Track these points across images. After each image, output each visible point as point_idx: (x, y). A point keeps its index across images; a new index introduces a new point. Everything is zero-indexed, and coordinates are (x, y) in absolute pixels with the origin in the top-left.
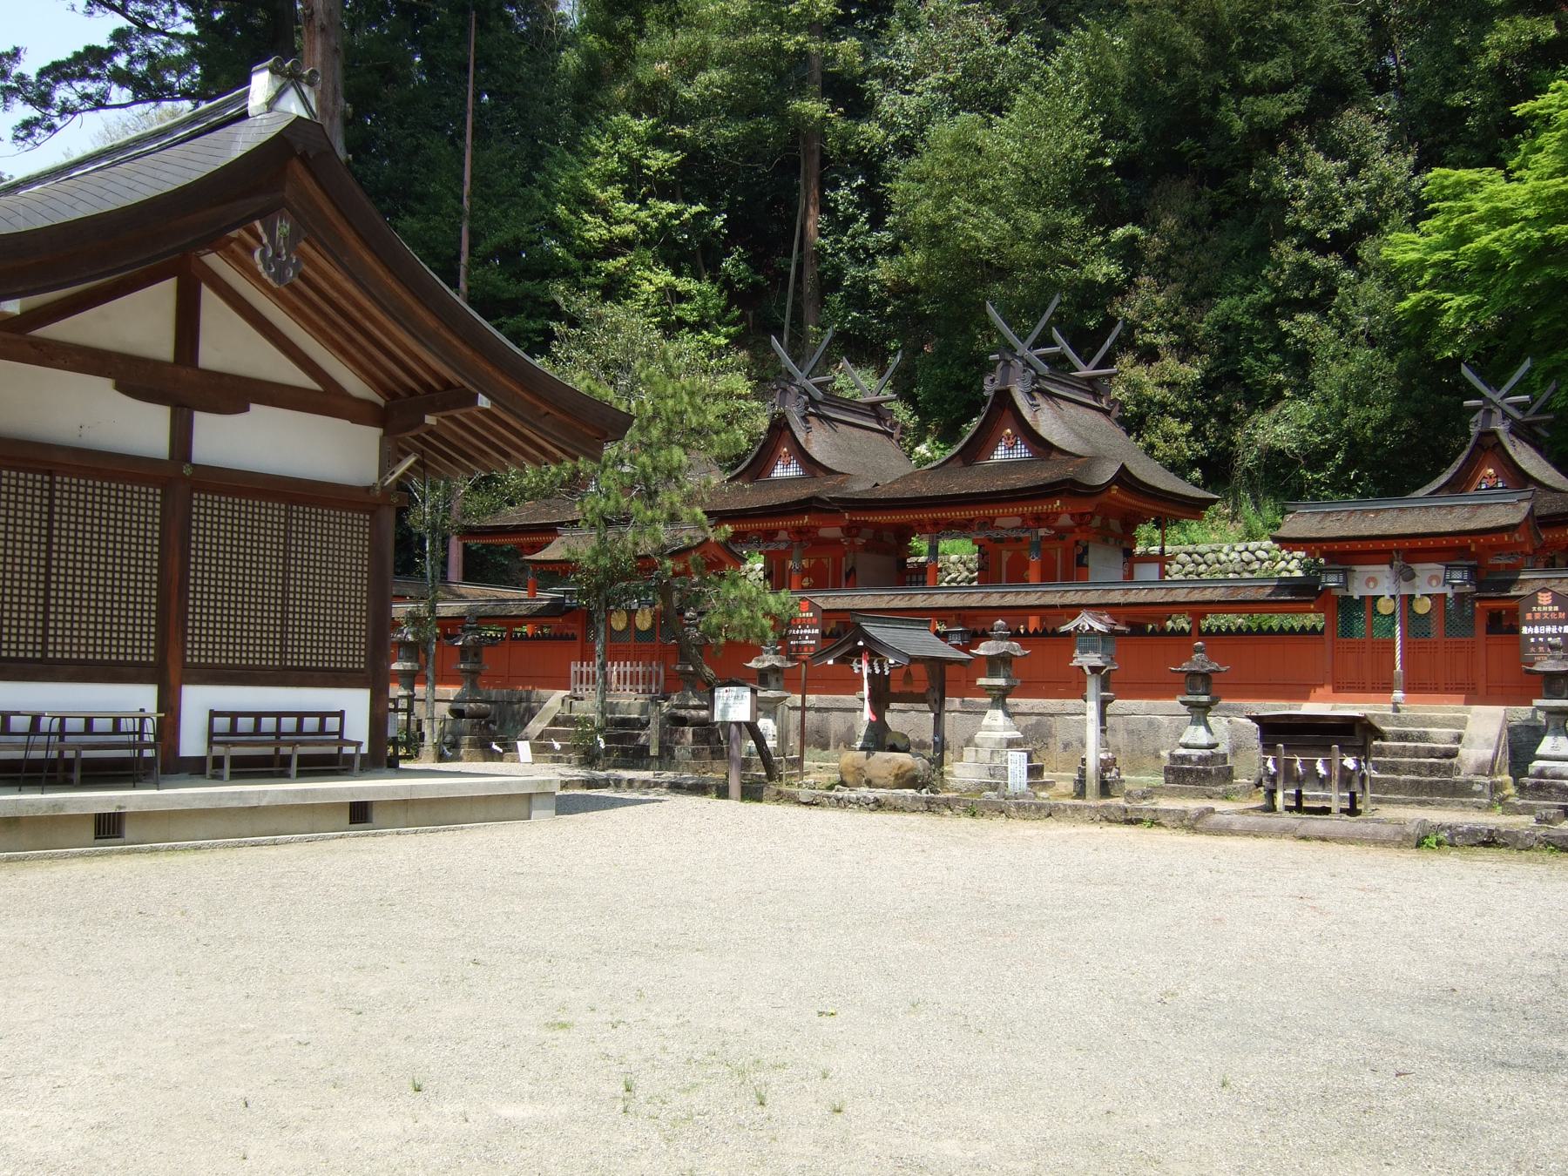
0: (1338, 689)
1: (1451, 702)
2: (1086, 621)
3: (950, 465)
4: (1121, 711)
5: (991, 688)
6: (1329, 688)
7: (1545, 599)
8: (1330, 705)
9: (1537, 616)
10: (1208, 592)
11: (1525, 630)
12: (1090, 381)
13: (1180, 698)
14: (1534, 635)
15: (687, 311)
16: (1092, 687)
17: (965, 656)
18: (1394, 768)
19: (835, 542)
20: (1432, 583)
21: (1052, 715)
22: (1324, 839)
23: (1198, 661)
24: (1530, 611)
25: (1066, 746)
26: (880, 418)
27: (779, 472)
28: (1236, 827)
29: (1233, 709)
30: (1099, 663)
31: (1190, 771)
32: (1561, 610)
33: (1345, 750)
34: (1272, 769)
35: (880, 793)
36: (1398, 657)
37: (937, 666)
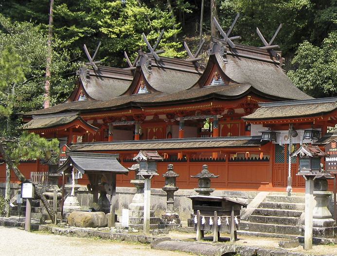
0: (274, 185)
2: (142, 156)
3: (194, 88)
5: (135, 184)
8: (268, 193)
12: (269, 50)
13: (195, 189)
14: (332, 162)
15: (156, 23)
17: (125, 170)
18: (276, 221)
19: (162, 121)
21: (180, 196)
23: (205, 172)
25: (184, 209)
26: (196, 69)
27: (141, 91)
29: (237, 194)
30: (146, 174)
33: (219, 214)
35: (73, 229)
36: (290, 170)
37: (114, 174)
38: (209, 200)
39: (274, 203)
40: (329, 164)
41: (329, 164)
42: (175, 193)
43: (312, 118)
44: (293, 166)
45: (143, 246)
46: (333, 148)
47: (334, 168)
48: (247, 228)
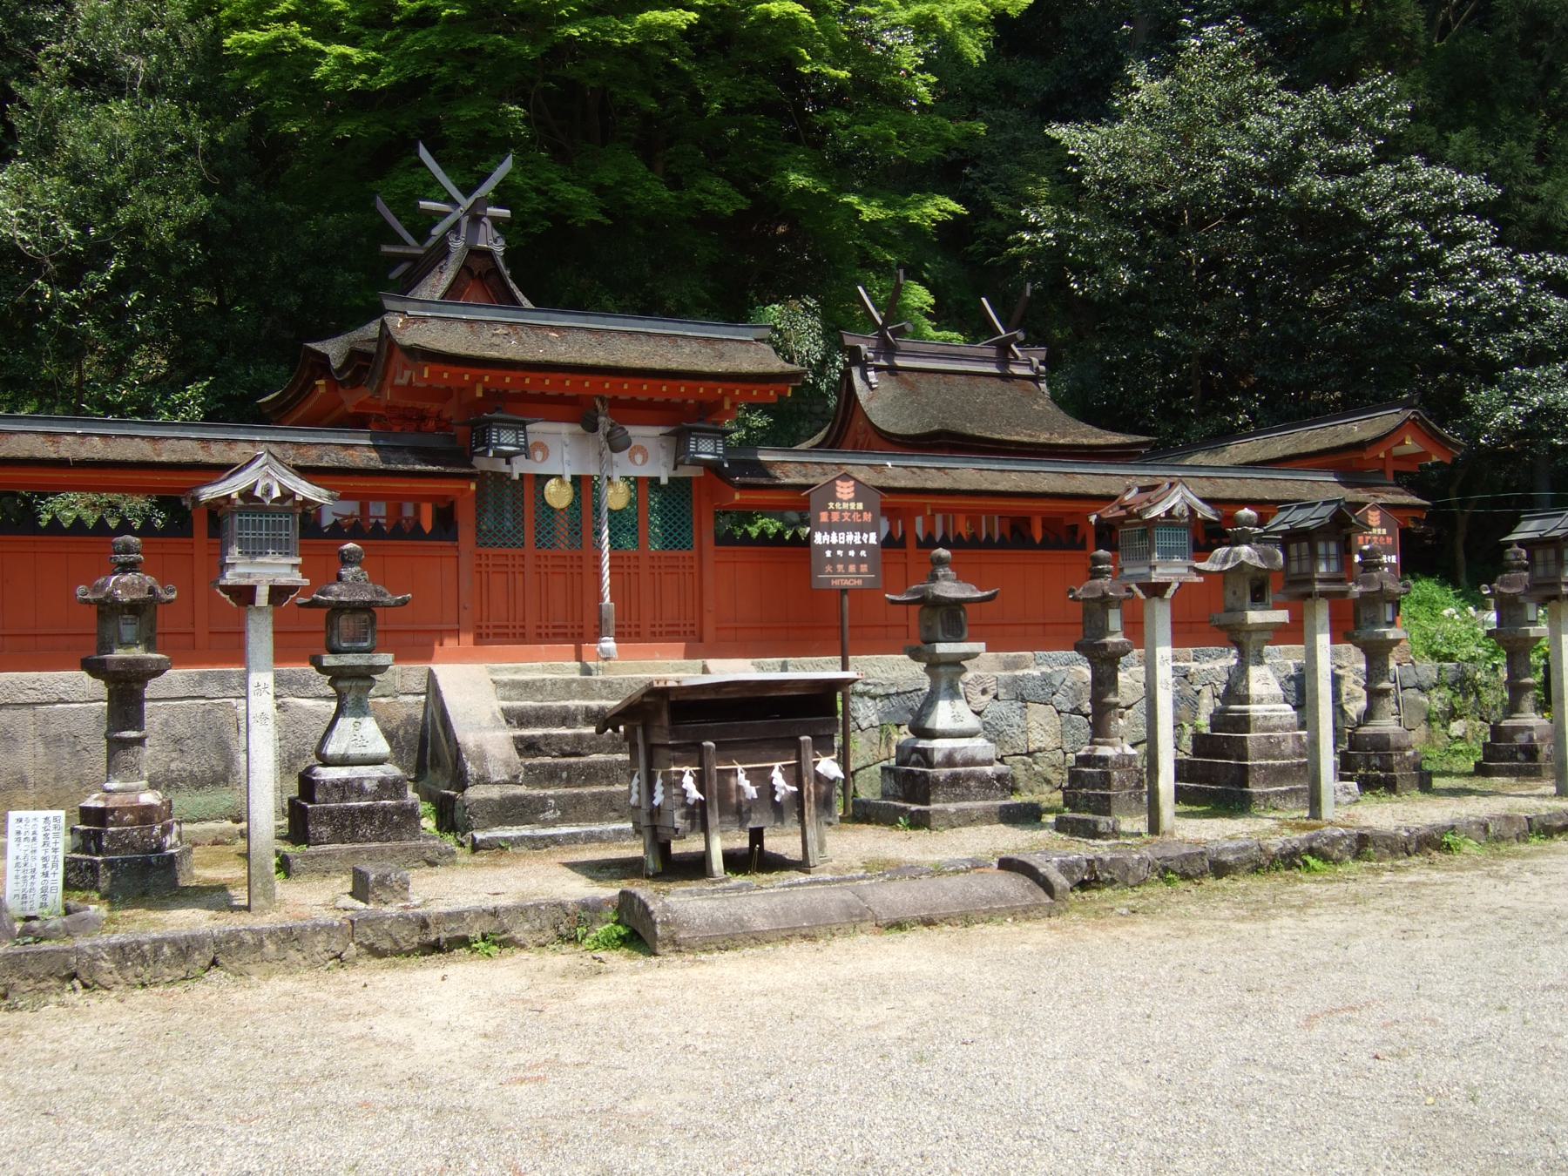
0: (480, 639)
1: (665, 654)
4: (33, 696)
6: (467, 638)
7: (845, 490)
9: (835, 517)
10: (215, 448)
11: (819, 538)
16: (260, 636)
20: (647, 456)
22: (929, 922)
24: (825, 508)
28: (760, 924)
30: (296, 578)
31: (367, 813)
32: (866, 509)
34: (694, 795)
38: (747, 694)
39: (572, 704)
40: (828, 554)
41: (828, 554)
42: (153, 688)
43: (748, 387)
44: (619, 562)
45: (896, 935)
46: (841, 501)
47: (846, 568)
48: (549, 815)
